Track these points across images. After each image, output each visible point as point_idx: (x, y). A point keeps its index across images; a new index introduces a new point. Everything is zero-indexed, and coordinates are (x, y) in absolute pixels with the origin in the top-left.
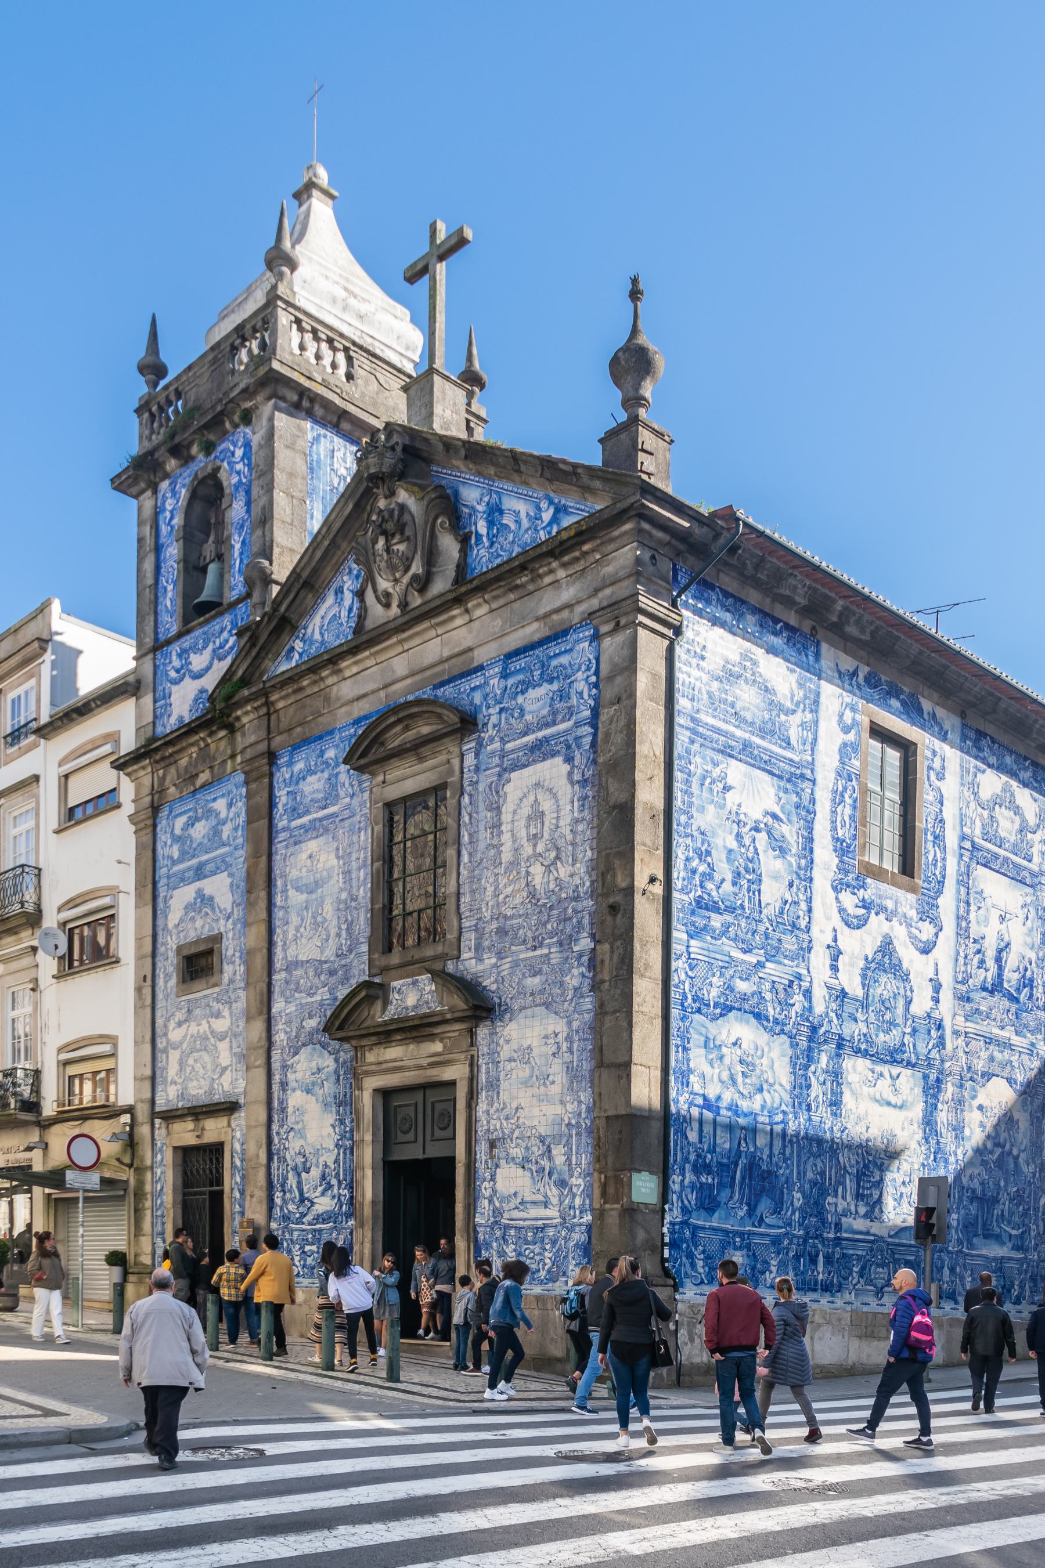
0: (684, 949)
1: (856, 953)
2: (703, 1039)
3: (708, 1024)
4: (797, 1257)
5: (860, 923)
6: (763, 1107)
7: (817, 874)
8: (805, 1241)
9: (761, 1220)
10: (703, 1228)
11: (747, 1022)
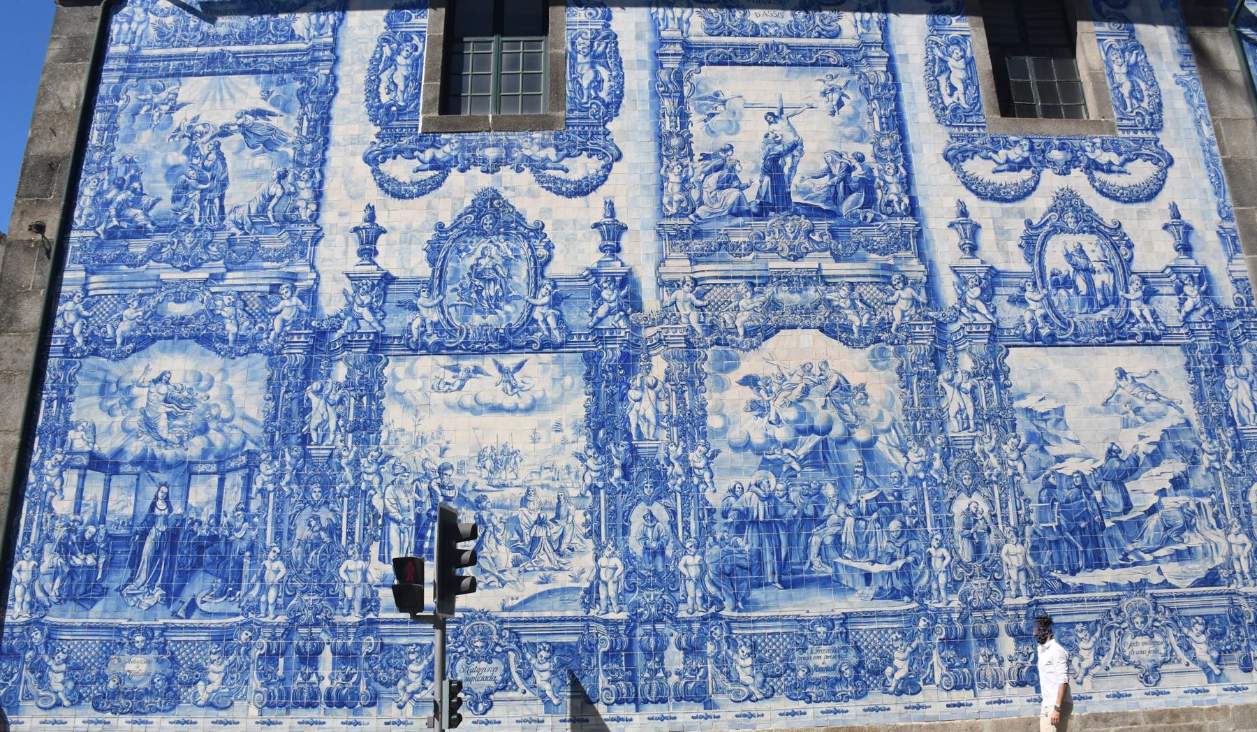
0: (79, 288)
1: (415, 225)
2: (98, 384)
4: (270, 657)
5: (423, 189)
6: (205, 453)
7: (332, 153)
8: (289, 632)
9: (191, 608)
10: (70, 628)
11: (184, 350)
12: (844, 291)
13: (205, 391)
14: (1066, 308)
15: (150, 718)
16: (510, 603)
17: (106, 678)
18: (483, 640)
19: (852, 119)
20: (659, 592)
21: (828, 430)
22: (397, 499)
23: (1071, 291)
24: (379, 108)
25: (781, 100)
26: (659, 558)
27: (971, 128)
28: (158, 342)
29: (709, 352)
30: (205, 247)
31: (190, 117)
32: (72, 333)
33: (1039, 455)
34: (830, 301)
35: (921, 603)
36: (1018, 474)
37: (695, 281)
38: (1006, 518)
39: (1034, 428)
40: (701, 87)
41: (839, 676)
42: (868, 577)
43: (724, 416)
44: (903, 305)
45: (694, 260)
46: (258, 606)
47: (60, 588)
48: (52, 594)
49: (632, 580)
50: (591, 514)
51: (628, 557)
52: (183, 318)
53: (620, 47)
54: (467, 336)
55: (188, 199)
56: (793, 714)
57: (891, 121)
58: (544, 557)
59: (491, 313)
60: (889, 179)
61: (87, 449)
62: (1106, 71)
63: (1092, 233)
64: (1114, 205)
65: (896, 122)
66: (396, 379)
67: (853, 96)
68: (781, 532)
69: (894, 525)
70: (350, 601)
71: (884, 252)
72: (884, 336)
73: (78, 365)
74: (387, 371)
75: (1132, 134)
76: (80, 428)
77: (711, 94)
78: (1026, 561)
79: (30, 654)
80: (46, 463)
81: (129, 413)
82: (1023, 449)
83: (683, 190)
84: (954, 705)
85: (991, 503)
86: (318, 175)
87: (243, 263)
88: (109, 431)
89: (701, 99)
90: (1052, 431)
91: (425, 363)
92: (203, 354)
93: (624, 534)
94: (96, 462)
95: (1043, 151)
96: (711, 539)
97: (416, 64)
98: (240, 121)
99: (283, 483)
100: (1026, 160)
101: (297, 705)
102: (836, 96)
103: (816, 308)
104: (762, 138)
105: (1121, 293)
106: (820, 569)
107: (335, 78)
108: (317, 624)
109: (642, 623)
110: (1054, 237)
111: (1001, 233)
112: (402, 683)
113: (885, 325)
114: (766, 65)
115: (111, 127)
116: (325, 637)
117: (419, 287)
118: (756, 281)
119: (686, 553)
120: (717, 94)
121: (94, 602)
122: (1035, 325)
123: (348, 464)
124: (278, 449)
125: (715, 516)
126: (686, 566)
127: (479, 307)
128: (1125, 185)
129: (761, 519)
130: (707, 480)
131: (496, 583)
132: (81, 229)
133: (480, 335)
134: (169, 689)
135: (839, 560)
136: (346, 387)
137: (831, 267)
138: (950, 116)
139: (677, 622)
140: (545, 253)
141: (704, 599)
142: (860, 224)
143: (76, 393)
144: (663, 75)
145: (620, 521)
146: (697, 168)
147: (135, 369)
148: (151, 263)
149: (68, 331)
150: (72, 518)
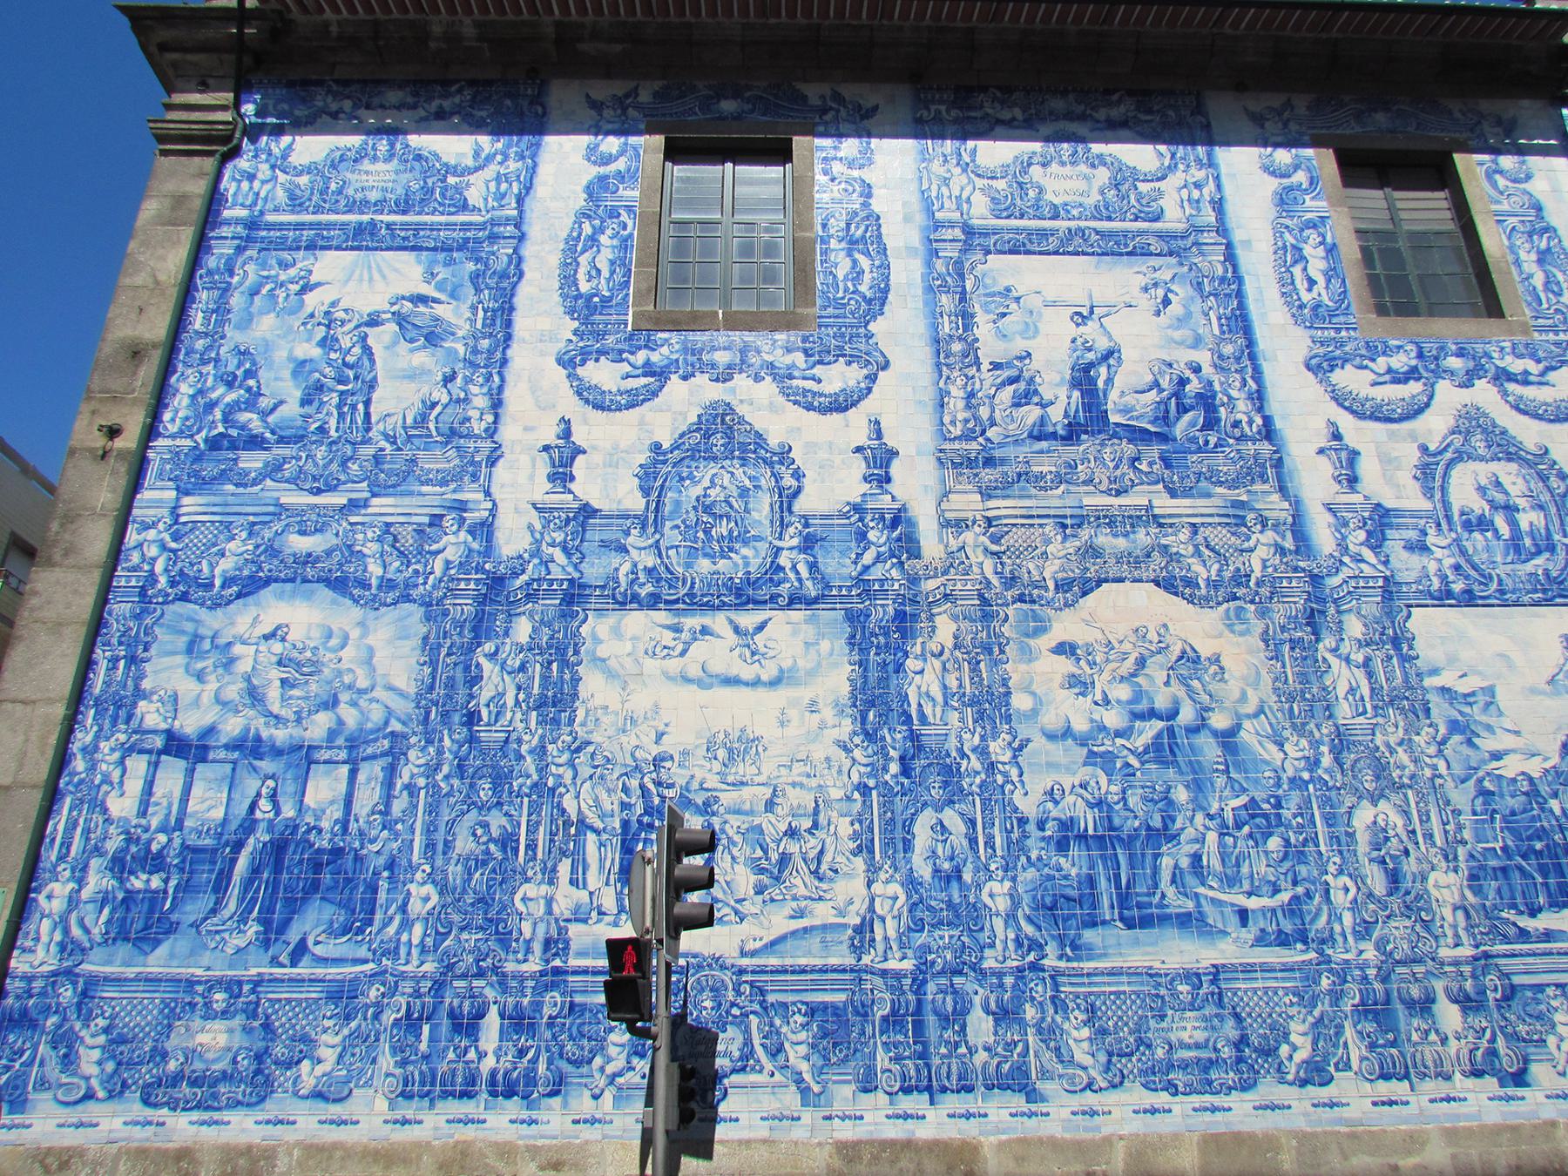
0: (165, 512)
1: (623, 445)
2: (185, 639)
3: (203, 614)
4: (410, 1023)
5: (634, 400)
6: (332, 734)
8: (439, 986)
9: (300, 951)
10: (118, 980)
11: (309, 596)
12: (1184, 535)
13: (336, 651)
14: (1485, 556)
15: (226, 1115)
16: (751, 946)
17: (165, 1055)
18: (714, 999)
19: (1181, 321)
20: (956, 933)
21: (1173, 714)
22: (596, 800)
23: (1489, 534)
24: (576, 298)
25: (1091, 297)
26: (955, 885)
27: (1338, 330)
28: (274, 585)
29: (1010, 611)
30: (344, 464)
31: (328, 301)
32: (152, 572)
33: (1466, 750)
34: (1166, 547)
35: (1321, 953)
36: (1440, 776)
37: (989, 521)
38: (1429, 836)
39: (1455, 715)
40: (988, 281)
41: (1214, 1056)
42: (1243, 915)
43: (1033, 694)
44: (1262, 552)
45: (986, 494)
46: (397, 948)
47: (109, 922)
48: (96, 931)
49: (919, 914)
50: (861, 822)
51: (911, 883)
52: (310, 555)
53: (883, 230)
54: (692, 587)
55: (322, 403)
56: (1153, 1111)
57: (1233, 323)
58: (798, 881)
59: (723, 557)
60: (1234, 394)
61: (164, 726)
62: (1510, 258)
63: (1509, 460)
64: (1535, 425)
65: (1240, 322)
66: (597, 640)
67: (1182, 292)
68: (1119, 851)
69: (1274, 843)
70: (528, 942)
71: (1233, 484)
72: (1240, 592)
73: (159, 612)
74: (584, 630)
75: (1551, 336)
76: (155, 697)
77: (1001, 289)
78: (1463, 896)
79: (53, 1020)
80: (102, 745)
81: (227, 678)
82: (1443, 742)
83: (968, 406)
84: (1383, 1103)
85: (1406, 814)
86: (496, 378)
87: (393, 486)
88: (197, 702)
89: (986, 295)
90: (1484, 719)
91: (637, 621)
92: (334, 602)
93: (905, 851)
94: (176, 745)
95: (1436, 358)
96: (1023, 859)
97: (625, 244)
98: (395, 308)
99: (439, 777)
100: (1414, 370)
101: (445, 1095)
102: (1160, 292)
103: (1148, 556)
104: (1068, 343)
105: (1556, 537)
106: (1177, 903)
107: (520, 260)
108: (481, 974)
109: (935, 976)
110: (1460, 467)
111: (1386, 460)
112: (598, 1061)
113: (1241, 578)
114: (1069, 253)
115: (221, 310)
116: (490, 994)
117: (629, 522)
118: (1068, 522)
119: (990, 878)
120: (1008, 290)
121: (157, 943)
122: (1444, 579)
123: (530, 752)
124: (435, 731)
125: (1028, 828)
126: (991, 895)
127: (708, 550)
128: (1549, 400)
129: (1091, 832)
130: (1015, 779)
131: (733, 917)
132: (173, 437)
133: (709, 585)
134: (258, 1072)
135: (1201, 890)
136: (531, 649)
137: (1164, 504)
138: (1312, 316)
139: (982, 974)
140: (794, 483)
141: (1018, 943)
142: (1199, 450)
143: (153, 651)
144: (940, 266)
145: (899, 834)
146: (986, 380)
147: (239, 620)
148: (269, 482)
149: (146, 567)
150: (134, 822)
